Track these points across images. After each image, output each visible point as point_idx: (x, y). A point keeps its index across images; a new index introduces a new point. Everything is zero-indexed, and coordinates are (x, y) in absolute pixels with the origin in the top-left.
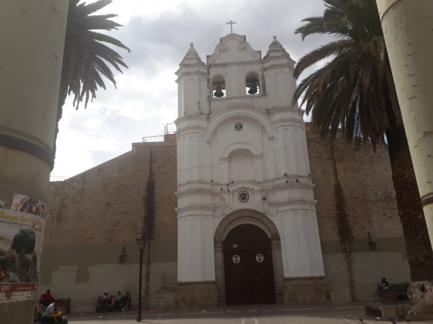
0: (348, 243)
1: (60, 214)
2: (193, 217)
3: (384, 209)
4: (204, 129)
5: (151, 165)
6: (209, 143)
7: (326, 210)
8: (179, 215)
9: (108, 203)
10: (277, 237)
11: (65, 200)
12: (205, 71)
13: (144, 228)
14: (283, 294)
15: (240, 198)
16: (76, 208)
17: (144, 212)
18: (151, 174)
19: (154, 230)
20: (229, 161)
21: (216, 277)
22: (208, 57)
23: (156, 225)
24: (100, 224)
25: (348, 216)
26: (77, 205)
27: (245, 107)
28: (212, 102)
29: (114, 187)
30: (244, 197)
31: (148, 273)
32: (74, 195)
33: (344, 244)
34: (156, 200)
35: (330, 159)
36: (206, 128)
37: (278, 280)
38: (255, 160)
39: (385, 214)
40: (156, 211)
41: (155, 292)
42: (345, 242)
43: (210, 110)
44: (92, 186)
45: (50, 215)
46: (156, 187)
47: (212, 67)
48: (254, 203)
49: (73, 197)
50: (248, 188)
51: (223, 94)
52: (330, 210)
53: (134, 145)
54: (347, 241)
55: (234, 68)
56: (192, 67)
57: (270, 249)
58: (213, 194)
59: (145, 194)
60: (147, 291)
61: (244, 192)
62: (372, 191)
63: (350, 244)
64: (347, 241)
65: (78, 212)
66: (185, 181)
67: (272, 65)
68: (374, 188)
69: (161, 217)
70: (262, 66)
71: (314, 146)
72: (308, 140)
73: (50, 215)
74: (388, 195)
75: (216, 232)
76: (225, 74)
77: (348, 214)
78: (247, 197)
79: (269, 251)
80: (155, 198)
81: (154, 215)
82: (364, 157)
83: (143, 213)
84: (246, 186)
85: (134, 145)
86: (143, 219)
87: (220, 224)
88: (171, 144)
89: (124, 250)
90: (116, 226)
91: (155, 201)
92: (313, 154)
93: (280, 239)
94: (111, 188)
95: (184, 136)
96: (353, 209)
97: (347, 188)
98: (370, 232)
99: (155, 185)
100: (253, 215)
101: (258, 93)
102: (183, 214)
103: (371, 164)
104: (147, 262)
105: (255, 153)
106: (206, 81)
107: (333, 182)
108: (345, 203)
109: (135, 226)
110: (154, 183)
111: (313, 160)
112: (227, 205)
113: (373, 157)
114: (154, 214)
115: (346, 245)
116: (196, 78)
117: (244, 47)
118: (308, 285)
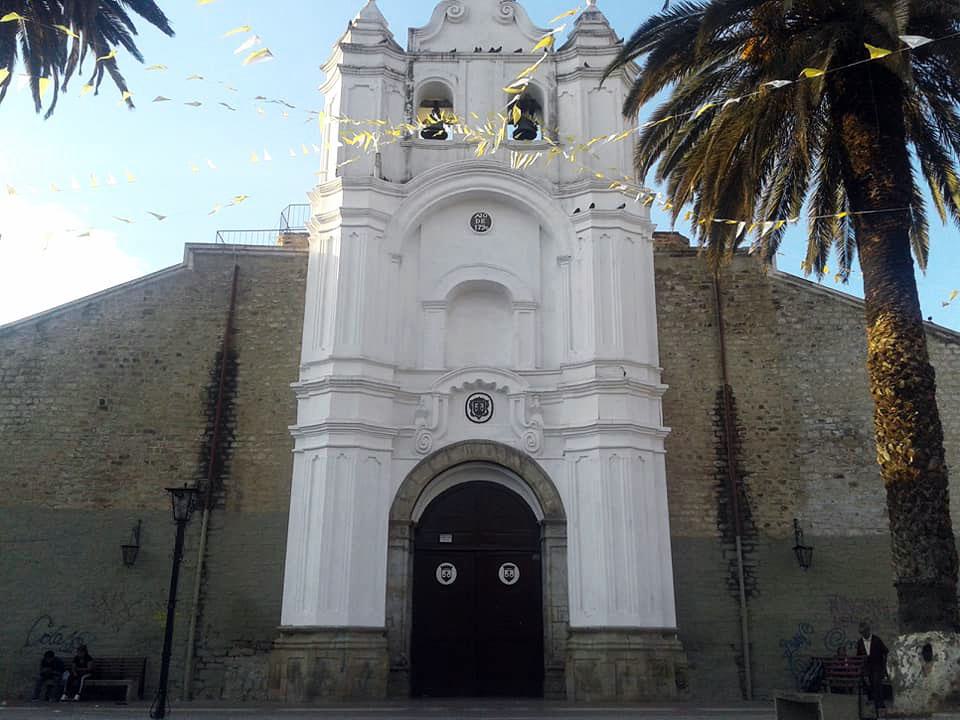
0: (743, 545)
2: (339, 451)
3: (838, 461)
4: (386, 219)
5: (232, 308)
6: (398, 258)
7: (690, 457)
8: (299, 446)
9: (102, 402)
10: (558, 519)
12: (402, 67)
14: (563, 670)
15: (469, 411)
16: (12, 407)
17: (203, 431)
18: (231, 330)
19: (225, 482)
20: (449, 313)
21: (387, 619)
22: (412, 31)
23: (232, 469)
24: (75, 458)
25: (747, 474)
26: (14, 401)
27: (503, 171)
28: (415, 150)
29: (125, 360)
30: (479, 409)
31: (200, 600)
32: (8, 373)
33: (731, 546)
35: (710, 325)
36: (390, 216)
37: (552, 631)
38: (517, 312)
39: (841, 477)
40: (235, 432)
41: (216, 653)
42: (735, 542)
43: (407, 172)
44: (62, 353)
46: (240, 367)
47: (422, 58)
48: (504, 428)
49: (6, 379)
50: (494, 384)
51: (444, 136)
52: (700, 457)
53: (193, 249)
54: (738, 538)
55: (478, 66)
56: (367, 52)
57: (539, 552)
58: (397, 394)
59: (209, 385)
60: (195, 648)
61: (481, 396)
62: (812, 415)
63: (748, 548)
64: (738, 538)
65: (18, 420)
66: (326, 355)
67: (579, 69)
68: (816, 407)
69: (247, 447)
70: (552, 67)
71: (673, 289)
72: (658, 272)
74: (851, 426)
75: (397, 496)
76: (454, 81)
77: (747, 469)
78: (490, 409)
79: (535, 557)
80: (236, 397)
81: (230, 442)
82: (798, 326)
83: (198, 435)
84: (488, 379)
85: (193, 249)
86: (199, 450)
87: (410, 477)
88: (294, 254)
89: (137, 531)
90: (120, 464)
91: (233, 404)
92: (668, 308)
93: (565, 523)
94: (117, 360)
95: (330, 234)
96: (759, 457)
97: (747, 402)
98: (800, 519)
99: (238, 361)
100: (501, 458)
101: (538, 138)
103: (813, 346)
104: (199, 570)
105: (519, 292)
106: (403, 93)
107: (714, 385)
108: (741, 442)
109: (172, 468)
110: (236, 357)
111: (667, 324)
112: (434, 426)
113: (820, 329)
114: (230, 439)
115: (735, 550)
116: (376, 82)
117: (511, 14)
118: (630, 650)
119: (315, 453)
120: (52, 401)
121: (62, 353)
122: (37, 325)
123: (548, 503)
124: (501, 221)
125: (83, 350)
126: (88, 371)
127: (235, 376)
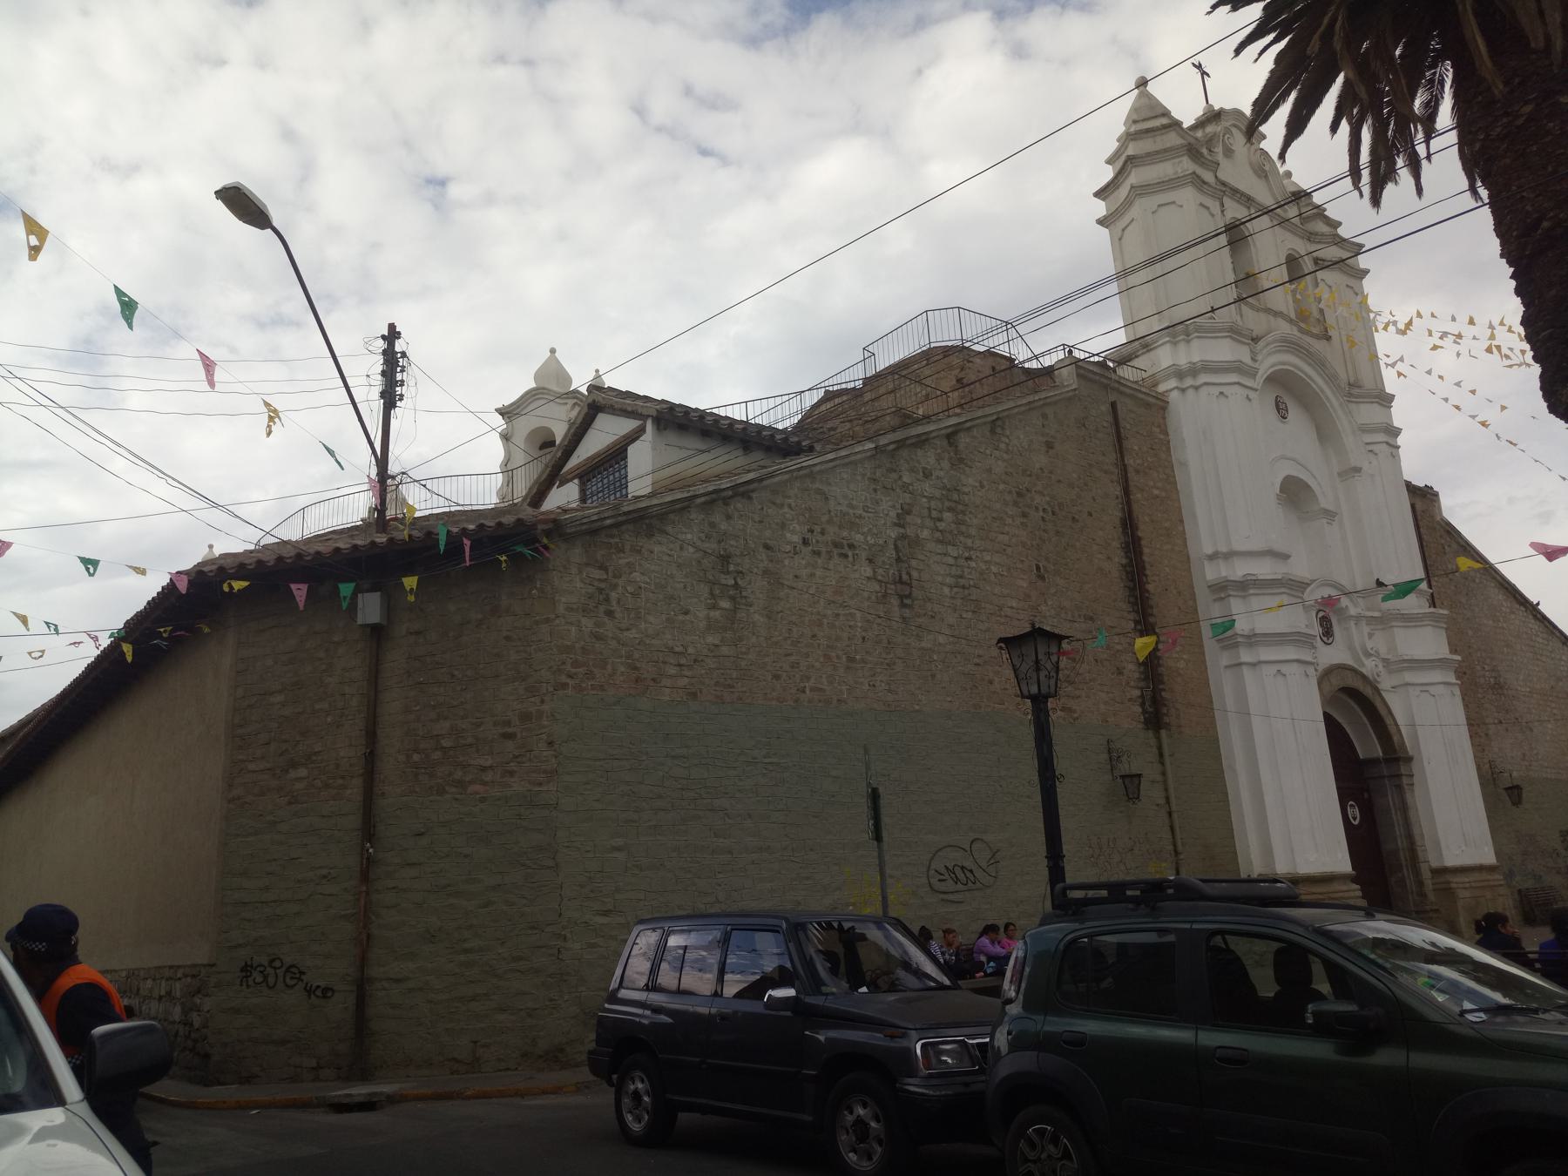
1: (905, 577)
9: (1038, 568)
11: (909, 519)
13: (1142, 684)
16: (951, 561)
18: (1127, 491)
26: (950, 548)
34: (1150, 587)
44: (982, 486)
45: (869, 572)
46: (1143, 542)
49: (934, 514)
59: (1124, 561)
65: (962, 582)
73: (869, 572)
102: (1266, 654)
119: (1273, 669)
120: (988, 558)
121: (982, 486)
122: (948, 436)
123: (1395, 738)
124: (1294, 412)
125: (1002, 487)
126: (1012, 517)
127: (1141, 553)
